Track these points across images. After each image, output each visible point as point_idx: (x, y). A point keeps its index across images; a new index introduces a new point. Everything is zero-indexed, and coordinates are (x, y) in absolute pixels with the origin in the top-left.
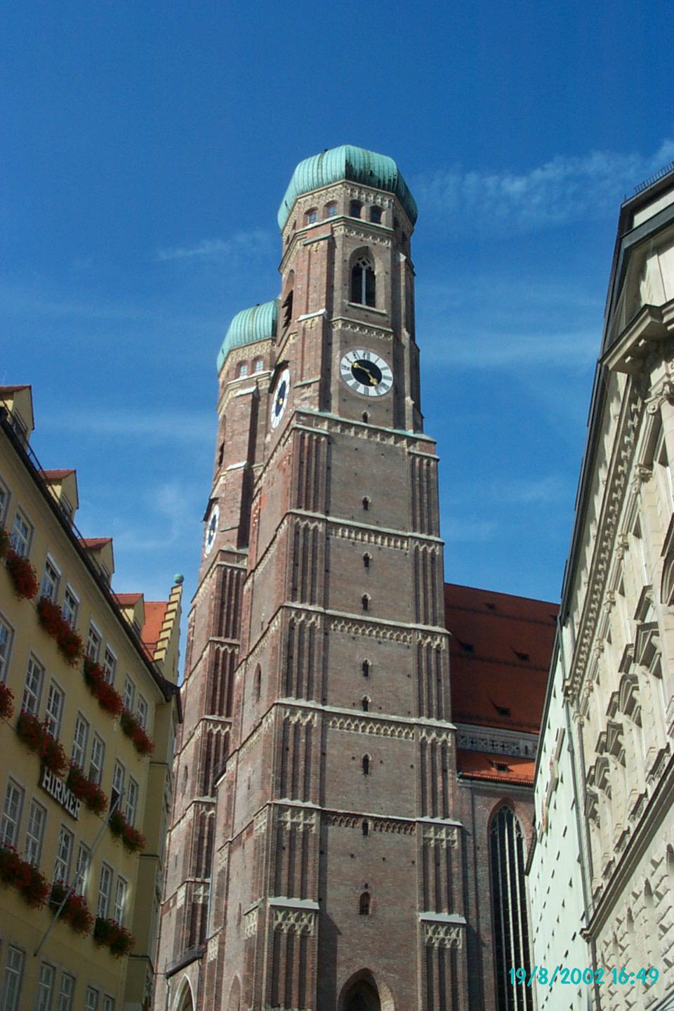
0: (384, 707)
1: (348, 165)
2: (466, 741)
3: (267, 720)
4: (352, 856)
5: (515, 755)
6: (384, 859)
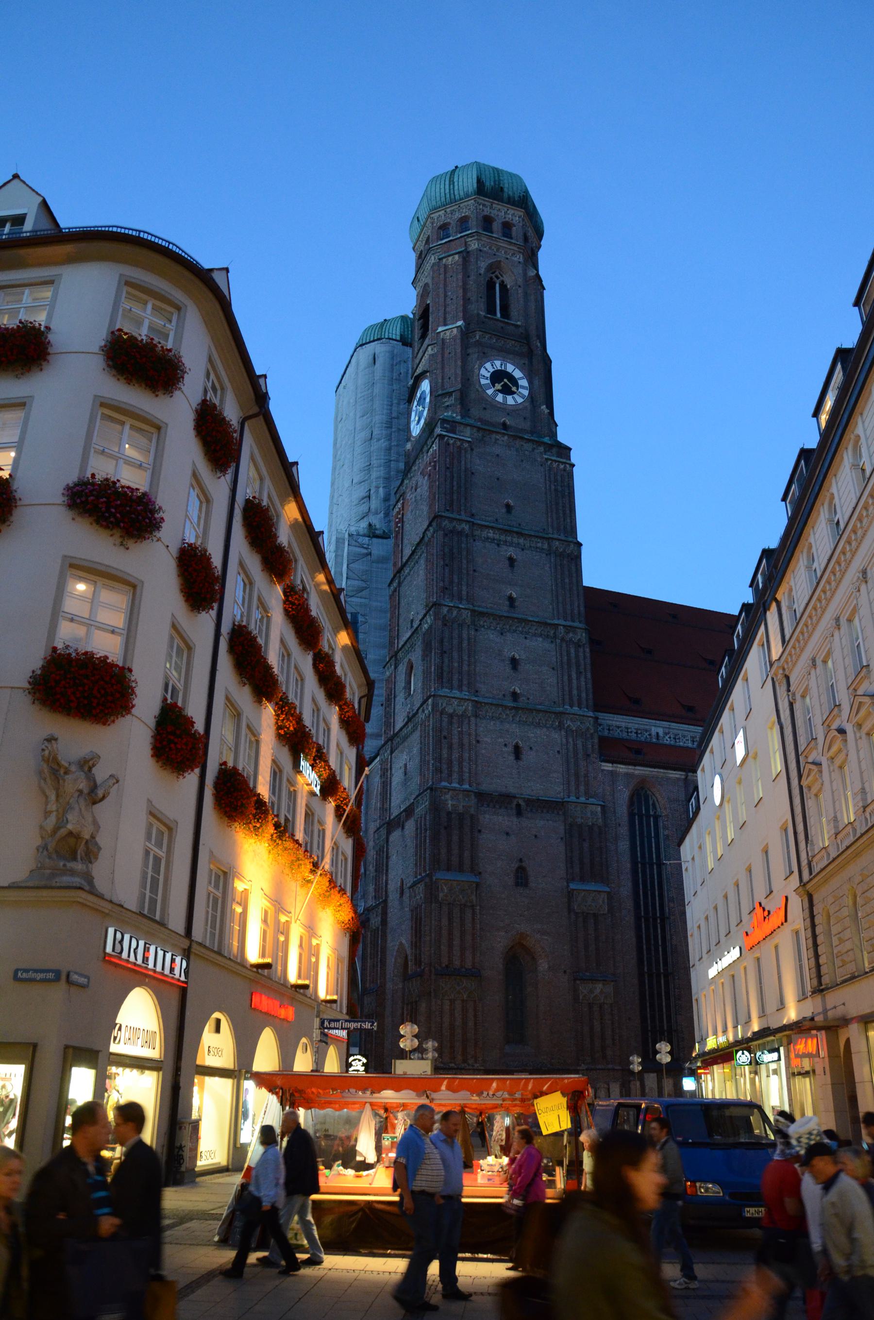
1: (479, 181)
2: (603, 729)
3: (423, 711)
4: (507, 834)
6: (536, 836)
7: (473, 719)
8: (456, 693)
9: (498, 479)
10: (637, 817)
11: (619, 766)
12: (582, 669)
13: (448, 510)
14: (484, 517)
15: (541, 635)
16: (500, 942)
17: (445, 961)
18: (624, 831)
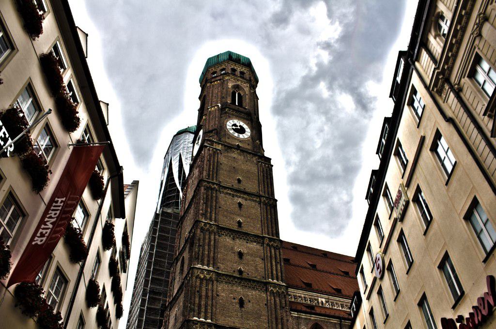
2: (291, 297)
3: (187, 279)
7: (215, 282)
8: (206, 267)
12: (278, 261)
15: (255, 242)
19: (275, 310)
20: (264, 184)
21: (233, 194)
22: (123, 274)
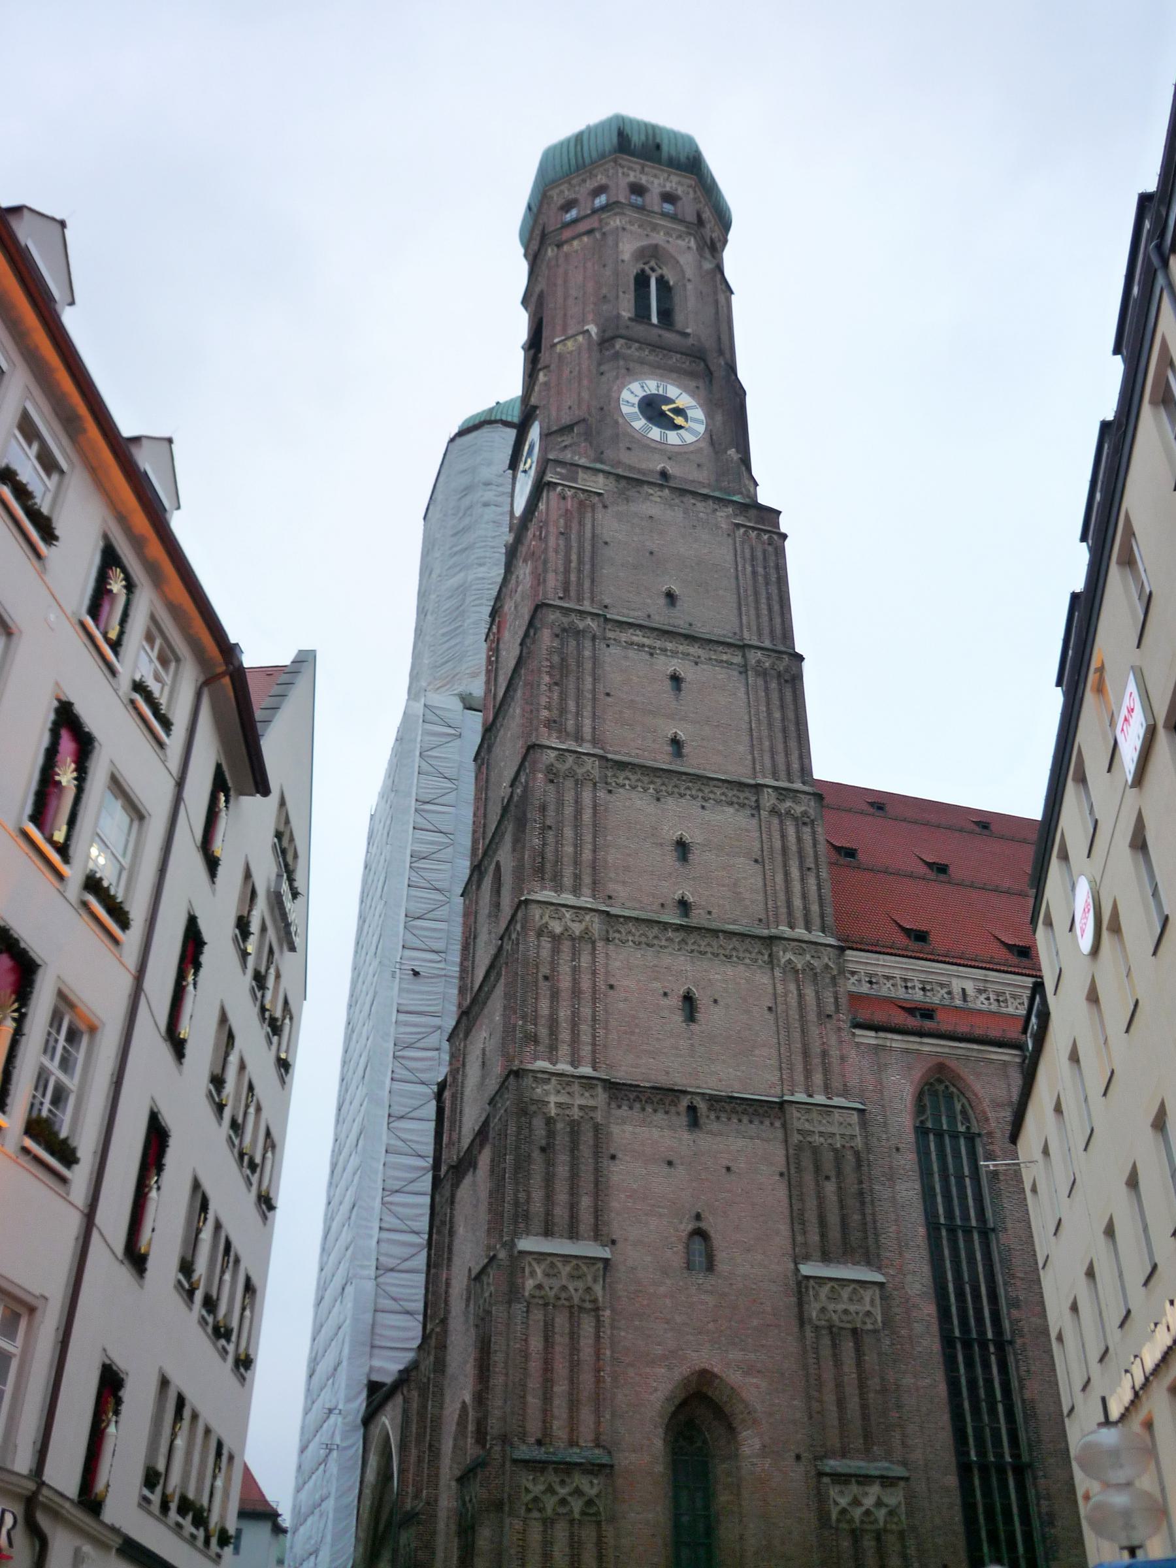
0: (714, 911)
1: (621, 134)
2: (859, 981)
3: (510, 938)
4: (670, 1163)
5: (947, 1002)
6: (728, 1169)
7: (600, 944)
9: (651, 553)
10: (931, 1137)
11: (890, 1036)
13: (560, 598)
14: (625, 611)
15: (731, 804)
16: (656, 1390)
17: (534, 1428)
18: (908, 1160)
19: (802, 1026)
20: (757, 602)
21: (650, 647)
22: (288, 955)
